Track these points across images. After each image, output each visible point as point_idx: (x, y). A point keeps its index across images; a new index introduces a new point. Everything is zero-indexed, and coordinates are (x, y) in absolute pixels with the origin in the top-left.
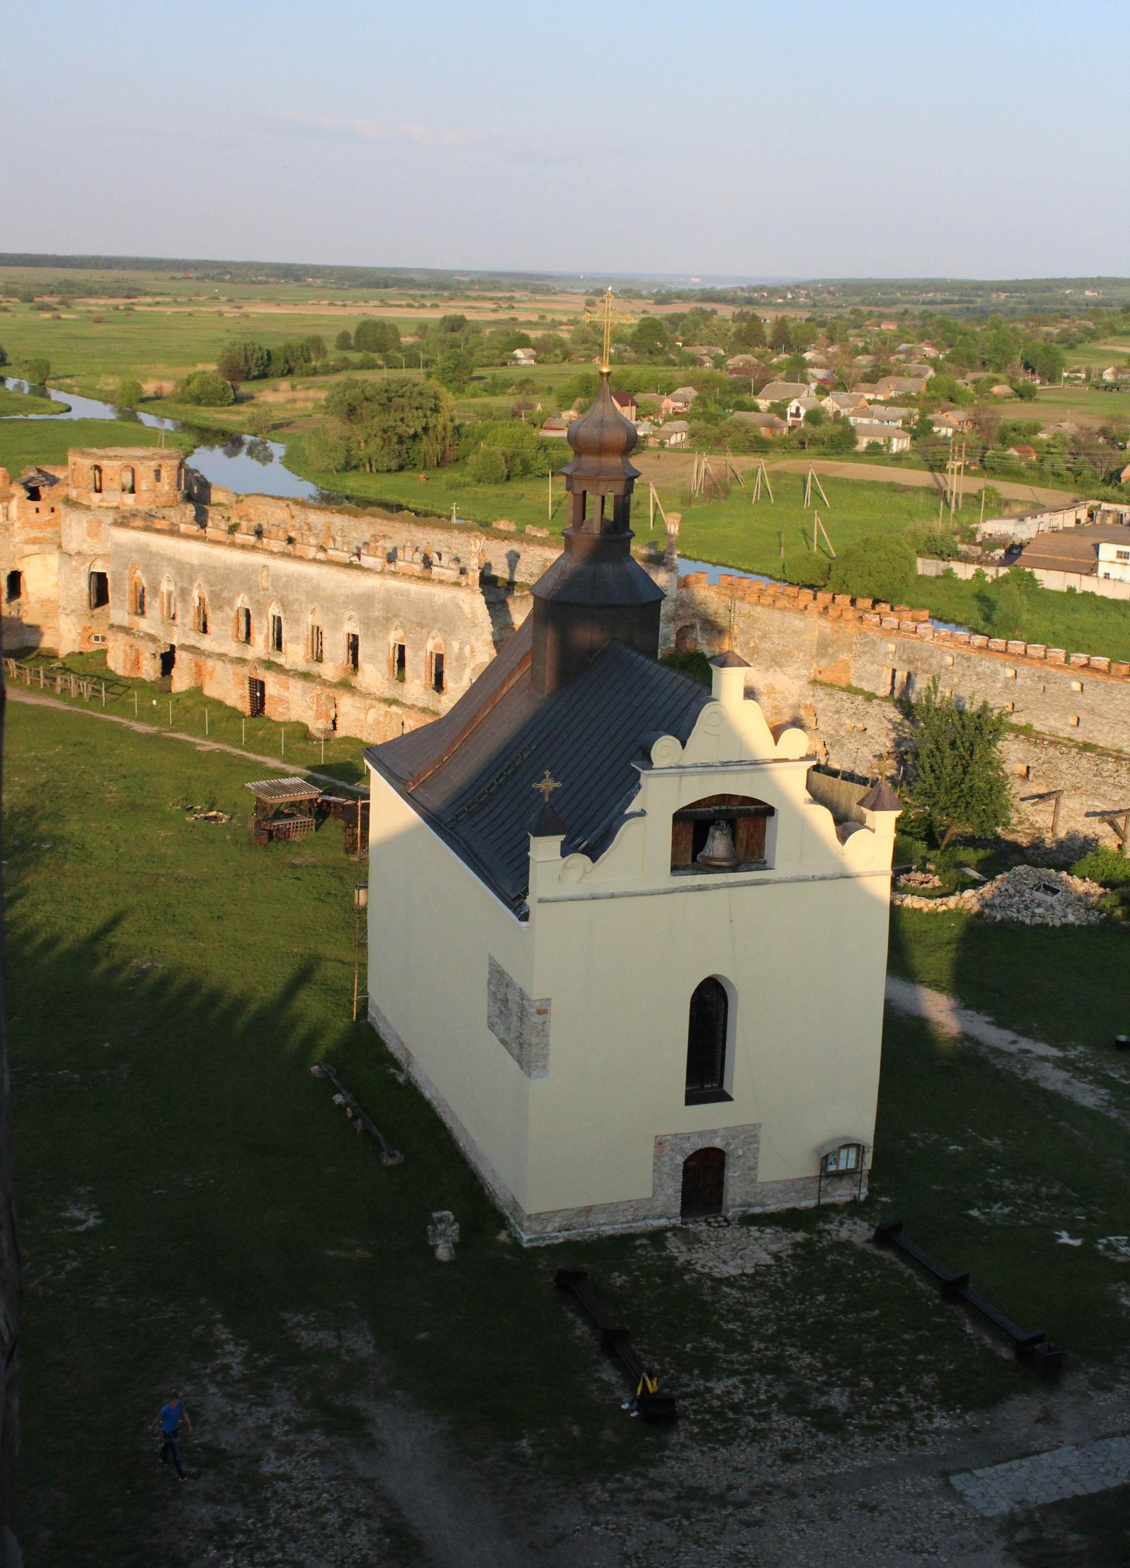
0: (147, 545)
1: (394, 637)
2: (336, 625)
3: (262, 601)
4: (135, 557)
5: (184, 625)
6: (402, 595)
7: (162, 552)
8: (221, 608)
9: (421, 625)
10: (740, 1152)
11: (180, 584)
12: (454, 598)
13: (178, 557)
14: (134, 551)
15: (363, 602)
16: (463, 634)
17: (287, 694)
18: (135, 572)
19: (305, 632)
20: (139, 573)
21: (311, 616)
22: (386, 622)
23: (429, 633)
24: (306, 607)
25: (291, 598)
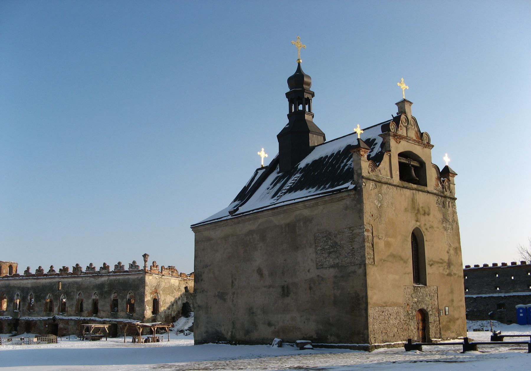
0: (9, 284)
1: (113, 296)
2: (89, 297)
3: (58, 295)
4: (4, 289)
5: (23, 310)
6: (117, 281)
7: (15, 286)
8: (40, 301)
10: (431, 312)
11: (22, 296)
12: (138, 277)
13: (22, 286)
14: (3, 287)
15: (100, 287)
17: (67, 326)
18: (3, 295)
19: (75, 302)
20: (5, 295)
21: (78, 296)
22: (109, 293)
23: (128, 293)
24: (76, 293)
25: (70, 291)
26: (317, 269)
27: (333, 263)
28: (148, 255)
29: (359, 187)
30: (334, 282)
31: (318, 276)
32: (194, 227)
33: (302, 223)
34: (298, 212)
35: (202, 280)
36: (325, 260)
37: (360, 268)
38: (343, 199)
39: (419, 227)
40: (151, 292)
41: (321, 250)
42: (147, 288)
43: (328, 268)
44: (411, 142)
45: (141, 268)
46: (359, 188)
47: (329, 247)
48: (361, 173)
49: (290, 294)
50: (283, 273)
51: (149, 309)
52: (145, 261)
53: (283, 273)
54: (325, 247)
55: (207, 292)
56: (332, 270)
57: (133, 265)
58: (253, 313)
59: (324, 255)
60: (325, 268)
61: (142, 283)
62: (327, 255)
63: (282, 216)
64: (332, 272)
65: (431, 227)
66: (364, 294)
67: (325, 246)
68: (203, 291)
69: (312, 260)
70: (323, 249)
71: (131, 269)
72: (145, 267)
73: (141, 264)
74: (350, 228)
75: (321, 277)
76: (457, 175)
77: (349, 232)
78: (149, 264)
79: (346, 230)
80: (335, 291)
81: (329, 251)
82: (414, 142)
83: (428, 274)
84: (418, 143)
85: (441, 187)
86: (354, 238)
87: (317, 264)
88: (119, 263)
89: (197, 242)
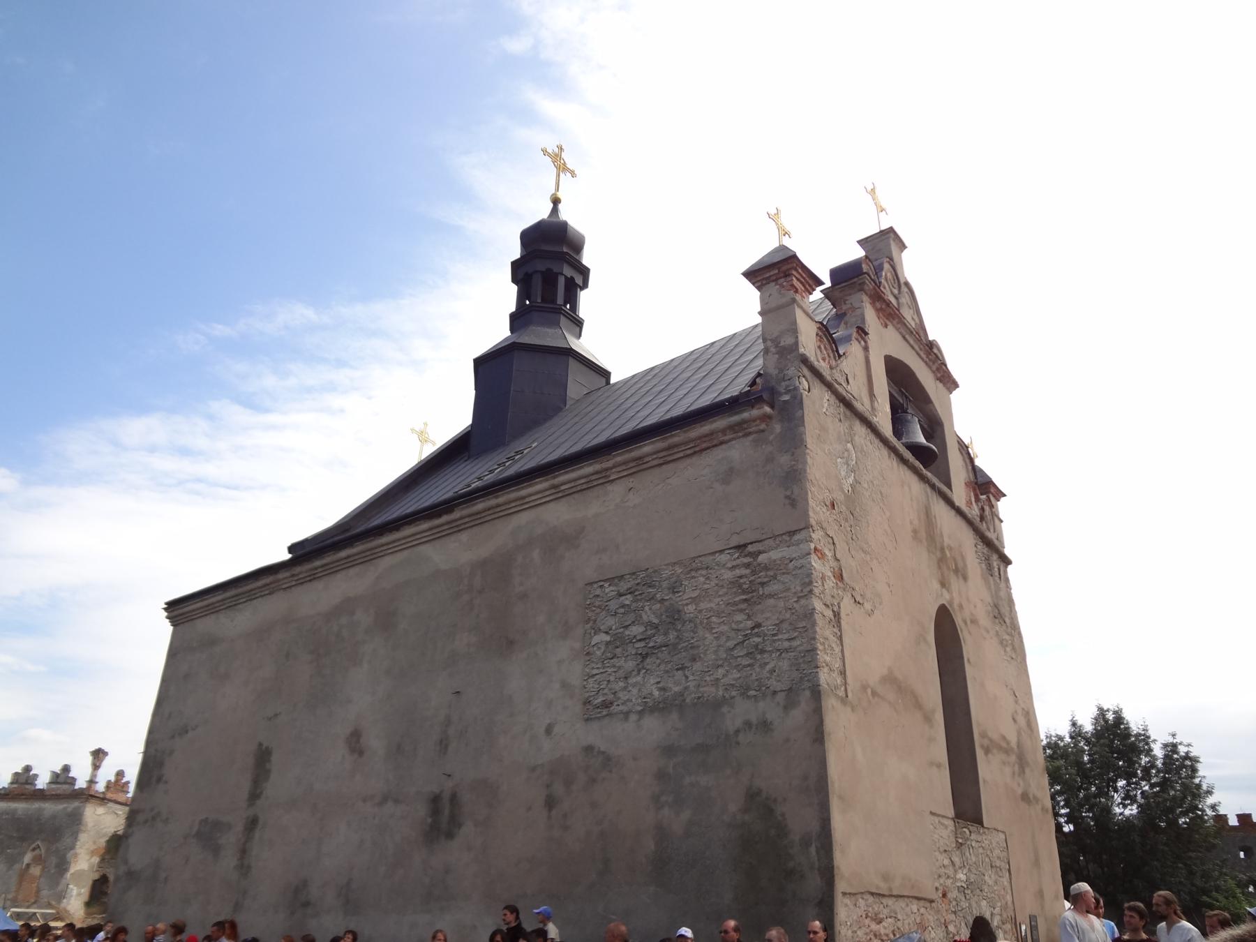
9: (22, 839)
12: (65, 808)
16: (68, 840)
26: (587, 720)
27: (656, 693)
28: (105, 754)
29: (788, 392)
30: (661, 776)
31: (589, 749)
32: (174, 607)
33: (536, 554)
34: (523, 518)
35: (159, 780)
36: (621, 684)
37: (790, 705)
38: (711, 443)
39: (948, 607)
40: (92, 848)
41: (608, 643)
42: (83, 837)
43: (633, 717)
44: (912, 342)
45: (81, 783)
46: (786, 398)
47: (641, 629)
48: (796, 344)
49: (460, 826)
50: (443, 745)
51: (79, 894)
52: (96, 767)
53: (443, 745)
54: (627, 633)
55: (166, 821)
56: (650, 722)
57: (63, 777)
58: (306, 904)
59: (621, 662)
60: (622, 716)
61: (75, 820)
62: (631, 664)
63: (464, 536)
64: (654, 729)
65: (974, 621)
66: (815, 826)
67: (626, 627)
68: (154, 818)
69: (565, 685)
70: (618, 641)
71: (53, 786)
72: (92, 782)
73: (81, 774)
74: (740, 547)
75: (603, 753)
76: (1004, 495)
77: (738, 562)
78: (106, 774)
79: (723, 558)
80: (666, 811)
81: (642, 644)
82: (919, 347)
83: (984, 781)
84: (927, 357)
85: (979, 514)
86: (763, 584)
87: (587, 702)
88: (28, 769)
89: (174, 654)
